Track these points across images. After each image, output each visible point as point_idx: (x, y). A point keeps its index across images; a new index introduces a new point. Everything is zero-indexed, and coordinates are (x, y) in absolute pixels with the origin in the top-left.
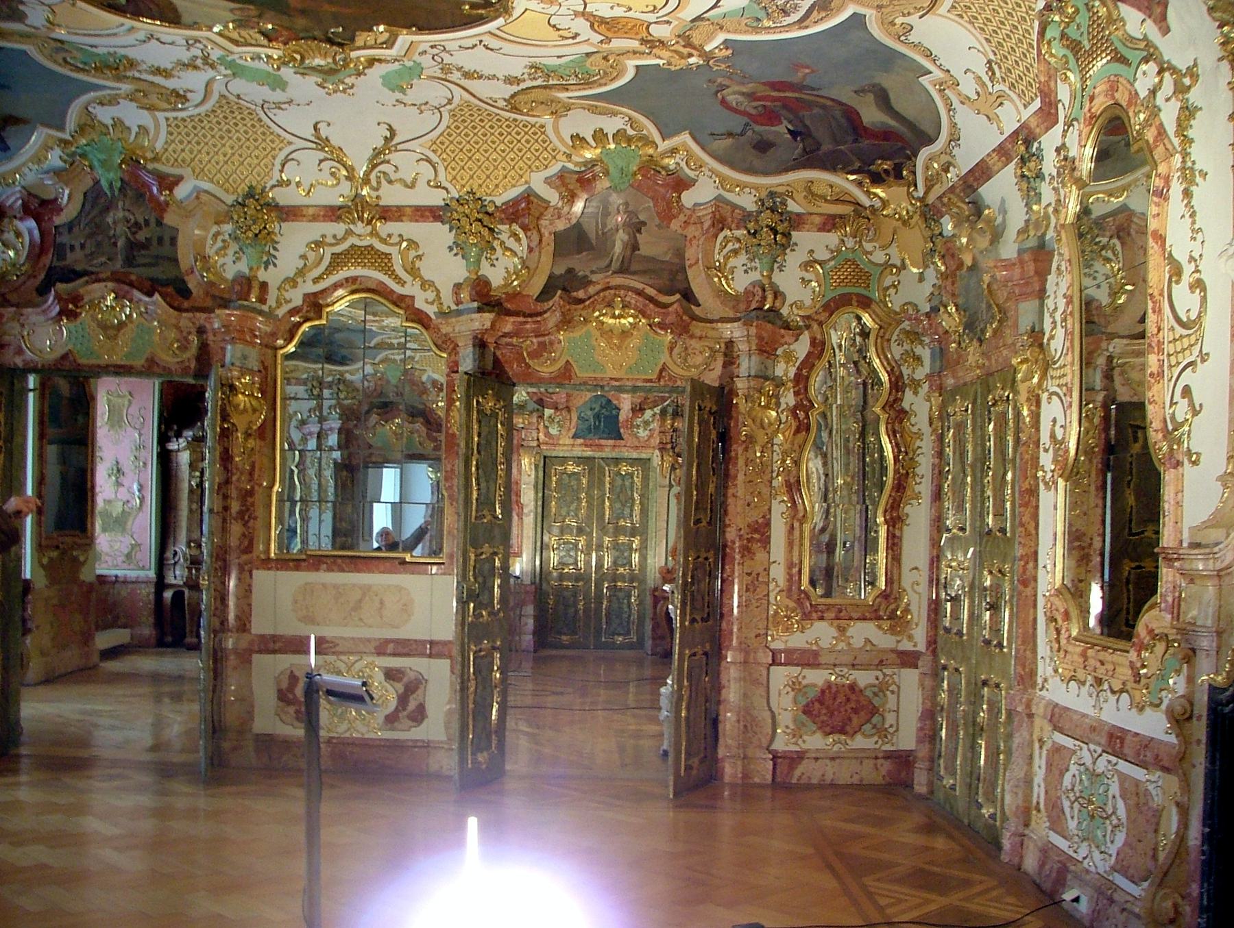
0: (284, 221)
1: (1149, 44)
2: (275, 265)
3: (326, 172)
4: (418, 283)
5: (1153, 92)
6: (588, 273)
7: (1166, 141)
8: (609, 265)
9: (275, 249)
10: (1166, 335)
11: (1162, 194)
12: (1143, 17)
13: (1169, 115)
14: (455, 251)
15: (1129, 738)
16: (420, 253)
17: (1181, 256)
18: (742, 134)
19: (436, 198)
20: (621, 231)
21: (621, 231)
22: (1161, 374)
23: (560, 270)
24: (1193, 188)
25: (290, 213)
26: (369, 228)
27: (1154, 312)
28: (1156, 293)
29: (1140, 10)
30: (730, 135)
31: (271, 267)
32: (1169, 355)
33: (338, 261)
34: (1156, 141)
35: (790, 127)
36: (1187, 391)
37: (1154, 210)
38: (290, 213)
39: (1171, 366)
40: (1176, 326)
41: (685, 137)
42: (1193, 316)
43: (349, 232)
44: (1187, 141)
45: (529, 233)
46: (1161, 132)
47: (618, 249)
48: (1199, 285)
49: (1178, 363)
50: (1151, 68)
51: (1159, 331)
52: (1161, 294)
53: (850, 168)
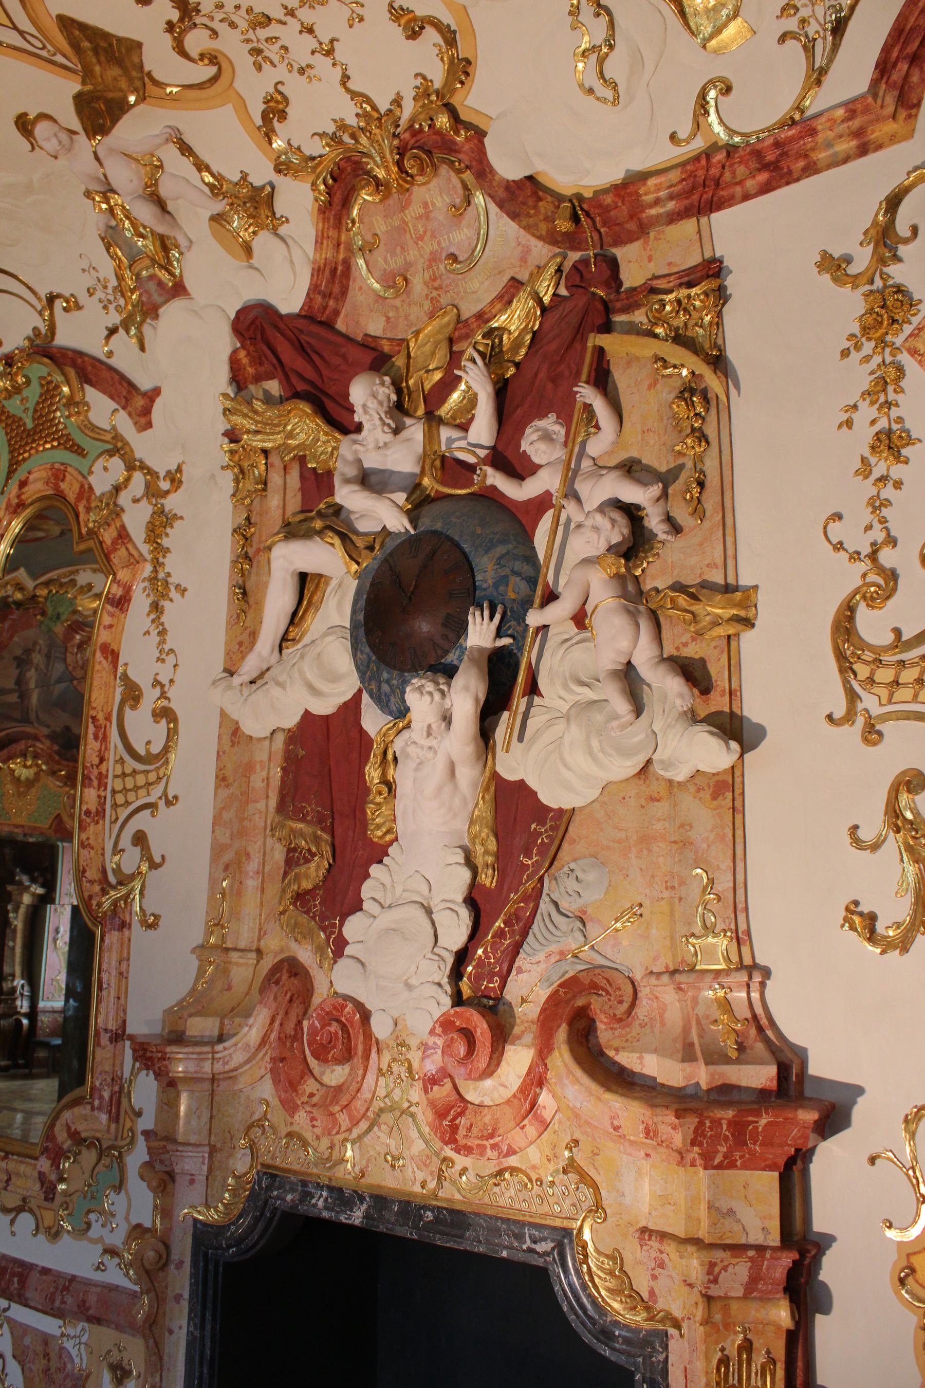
1: (117, 437)
5: (117, 489)
7: (130, 546)
10: (111, 767)
11: (121, 603)
12: (116, 406)
13: (136, 518)
15: (34, 1276)
17: (141, 675)
22: (101, 813)
24: (165, 604)
27: (96, 737)
28: (101, 716)
29: (112, 397)
32: (114, 792)
34: (114, 542)
36: (140, 839)
37: (107, 620)
39: (115, 806)
40: (127, 757)
42: (156, 749)
44: (160, 551)
46: (123, 535)
48: (165, 714)
49: (127, 803)
50: (117, 465)
51: (102, 760)
52: (108, 718)
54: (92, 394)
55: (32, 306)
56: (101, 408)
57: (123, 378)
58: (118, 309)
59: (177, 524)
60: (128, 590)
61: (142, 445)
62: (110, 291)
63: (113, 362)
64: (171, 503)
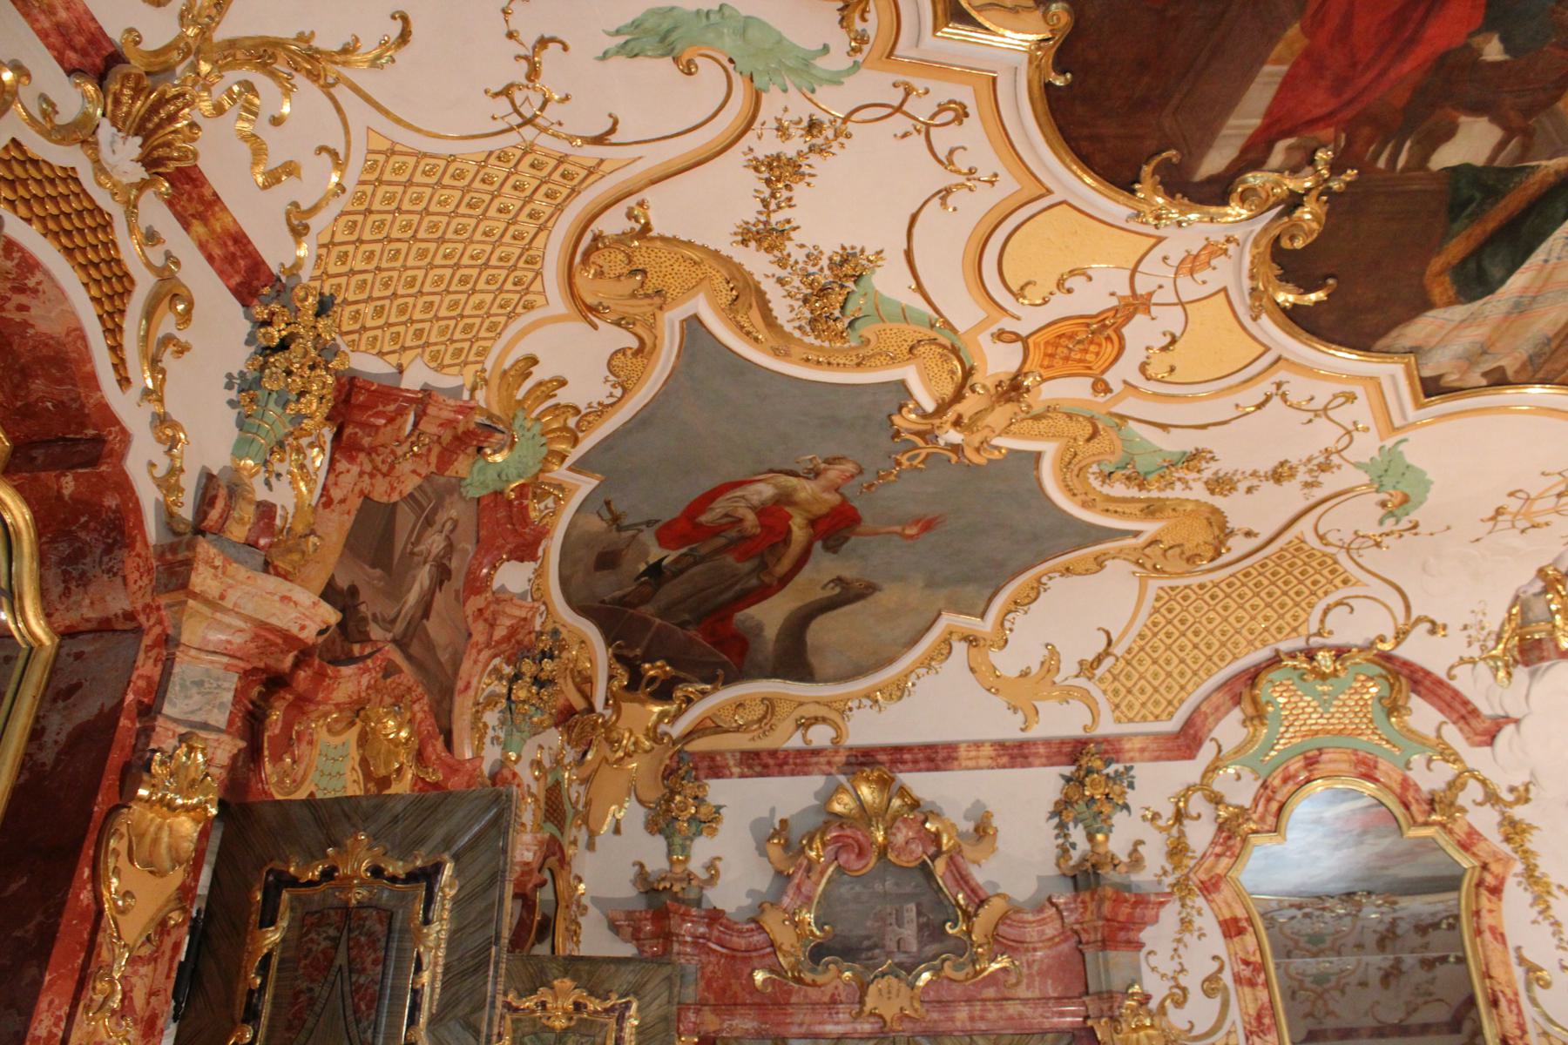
8: (393, 621)
11: (1496, 891)
12: (1443, 718)
13: (1485, 820)
14: (233, 394)
16: (182, 336)
18: (619, 529)
19: (276, 250)
20: (427, 567)
21: (427, 567)
24: (1550, 899)
30: (616, 519)
35: (665, 562)
41: (586, 485)
45: (342, 465)
47: (413, 597)
53: (625, 652)
54: (1415, 702)
55: (1394, 618)
56: (1423, 715)
57: (1466, 703)
58: (1483, 648)
59: (1534, 832)
60: (1502, 881)
61: (1476, 757)
62: (1485, 632)
63: (1454, 684)
64: (1519, 812)
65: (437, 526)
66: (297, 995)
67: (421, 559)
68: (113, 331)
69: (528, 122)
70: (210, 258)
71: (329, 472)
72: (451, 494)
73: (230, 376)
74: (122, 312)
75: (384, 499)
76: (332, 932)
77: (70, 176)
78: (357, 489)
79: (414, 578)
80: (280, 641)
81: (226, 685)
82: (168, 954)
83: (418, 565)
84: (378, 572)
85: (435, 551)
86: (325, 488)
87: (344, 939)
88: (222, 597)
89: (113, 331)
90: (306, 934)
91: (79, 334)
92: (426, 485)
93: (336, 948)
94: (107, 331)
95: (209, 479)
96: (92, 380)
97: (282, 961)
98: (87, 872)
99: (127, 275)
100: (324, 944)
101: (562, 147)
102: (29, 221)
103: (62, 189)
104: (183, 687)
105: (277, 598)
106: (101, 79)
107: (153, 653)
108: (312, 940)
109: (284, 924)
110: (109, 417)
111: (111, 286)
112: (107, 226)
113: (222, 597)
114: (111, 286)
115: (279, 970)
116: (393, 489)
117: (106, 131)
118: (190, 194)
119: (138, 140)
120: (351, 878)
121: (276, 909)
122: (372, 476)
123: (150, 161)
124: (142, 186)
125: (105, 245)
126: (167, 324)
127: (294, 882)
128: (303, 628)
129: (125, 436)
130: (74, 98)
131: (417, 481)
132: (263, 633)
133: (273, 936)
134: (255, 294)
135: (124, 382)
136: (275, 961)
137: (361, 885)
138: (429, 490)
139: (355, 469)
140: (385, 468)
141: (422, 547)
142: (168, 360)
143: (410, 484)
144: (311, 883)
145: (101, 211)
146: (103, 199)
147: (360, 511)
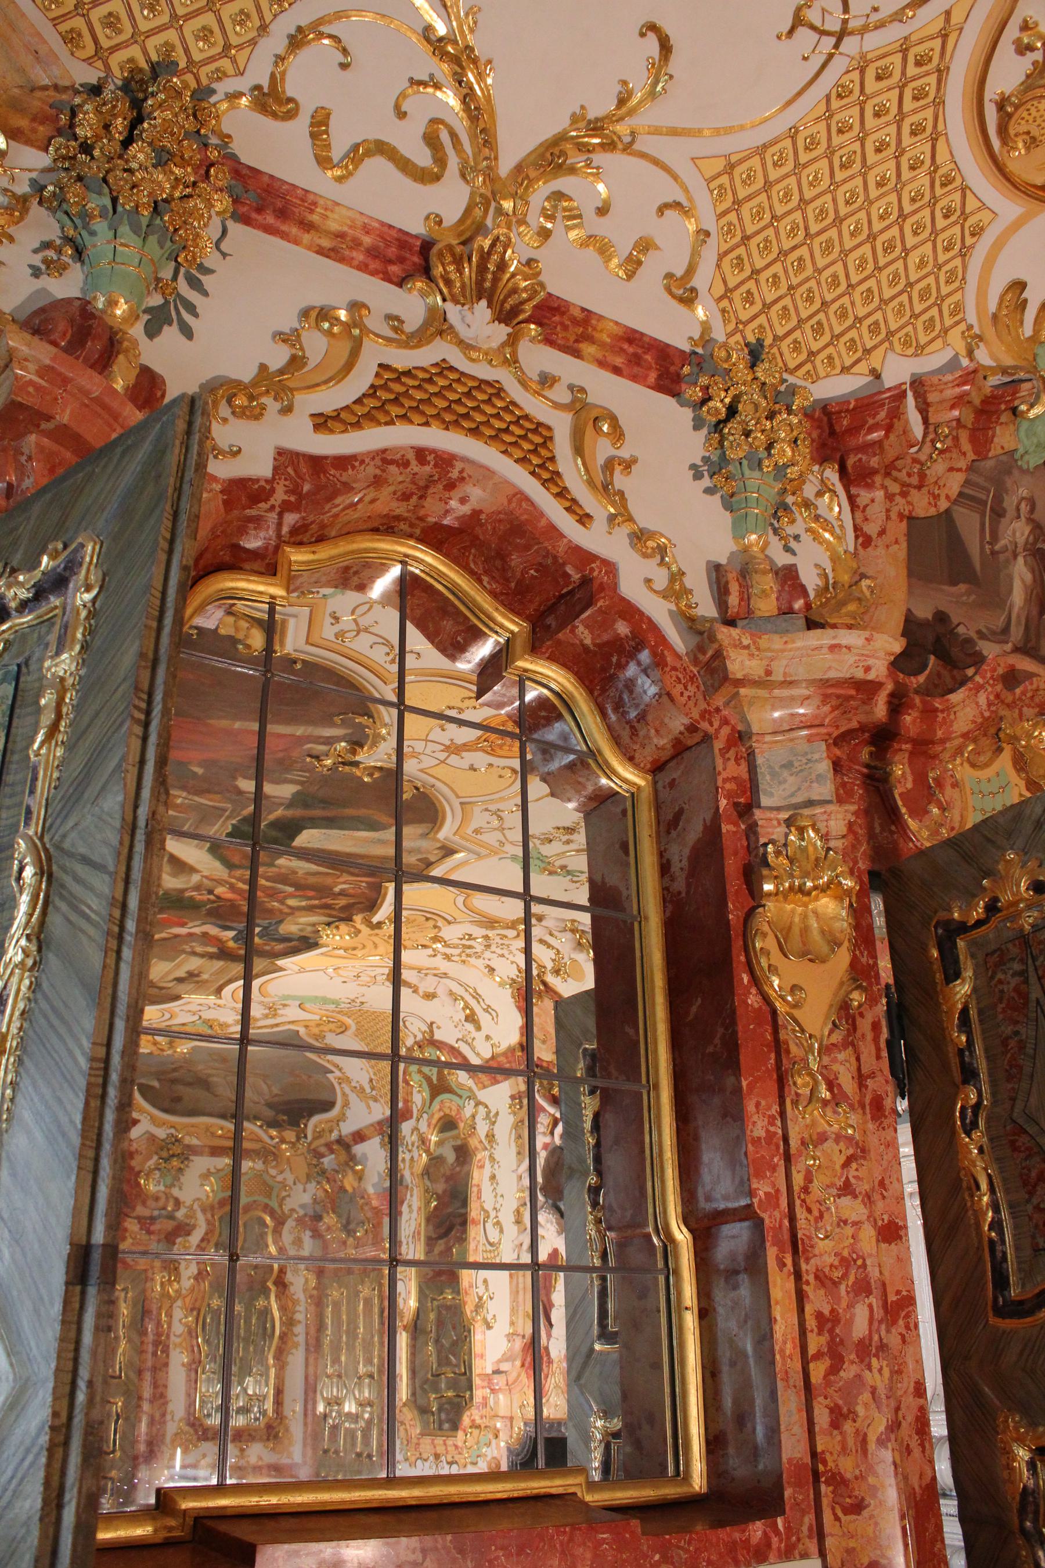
0: (246, 221)
2: (188, 332)
3: (416, 126)
4: (622, 532)
6: (974, 636)
8: (1006, 630)
9: (195, 284)
14: (706, 482)
16: (625, 453)
19: (676, 328)
20: (1020, 560)
21: (1020, 560)
23: (924, 612)
25: (268, 204)
26: (502, 331)
31: (171, 333)
33: (393, 396)
38: (268, 204)
43: (437, 326)
45: (864, 496)
65: (1011, 512)
66: (1005, 1042)
67: (1009, 554)
68: (552, 480)
69: (840, 36)
70: (617, 371)
71: (852, 511)
72: (1009, 473)
73: (693, 467)
74: (552, 459)
75: (932, 511)
76: (1017, 966)
77: (444, 368)
78: (894, 515)
79: (1011, 578)
80: (853, 692)
81: (816, 756)
82: (869, 1036)
83: (1007, 561)
84: (962, 587)
85: (1021, 540)
86: (856, 528)
87: (1031, 969)
88: (768, 673)
89: (552, 480)
90: (992, 978)
91: (521, 497)
92: (974, 478)
93: (1026, 981)
94: (544, 483)
95: (716, 570)
96: (553, 531)
97: (980, 1012)
98: (746, 978)
99: (540, 424)
100: (1014, 981)
101: (895, 33)
102: (427, 424)
103: (442, 382)
104: (774, 775)
105: (825, 650)
106: (426, 271)
107: (731, 754)
108: (1000, 982)
109: (968, 973)
110: (584, 557)
111: (531, 443)
112: (499, 392)
113: (768, 673)
114: (531, 443)
115: (981, 1022)
116: (937, 497)
117: (453, 312)
118: (561, 323)
119: (484, 303)
120: (1016, 903)
121: (956, 961)
122: (904, 494)
123: (506, 316)
124: (512, 341)
125: (506, 409)
126: (603, 450)
127: (962, 928)
128: (867, 669)
129: (610, 567)
130: (412, 304)
131: (958, 478)
132: (830, 691)
133: (963, 989)
134: (678, 379)
135: (585, 519)
136: (973, 1013)
137: (1029, 907)
138: (981, 480)
139: (879, 494)
140: (914, 480)
141: (1002, 543)
142: (620, 481)
143: (954, 484)
144: (979, 923)
145: (488, 383)
146: (483, 371)
147: (909, 535)
